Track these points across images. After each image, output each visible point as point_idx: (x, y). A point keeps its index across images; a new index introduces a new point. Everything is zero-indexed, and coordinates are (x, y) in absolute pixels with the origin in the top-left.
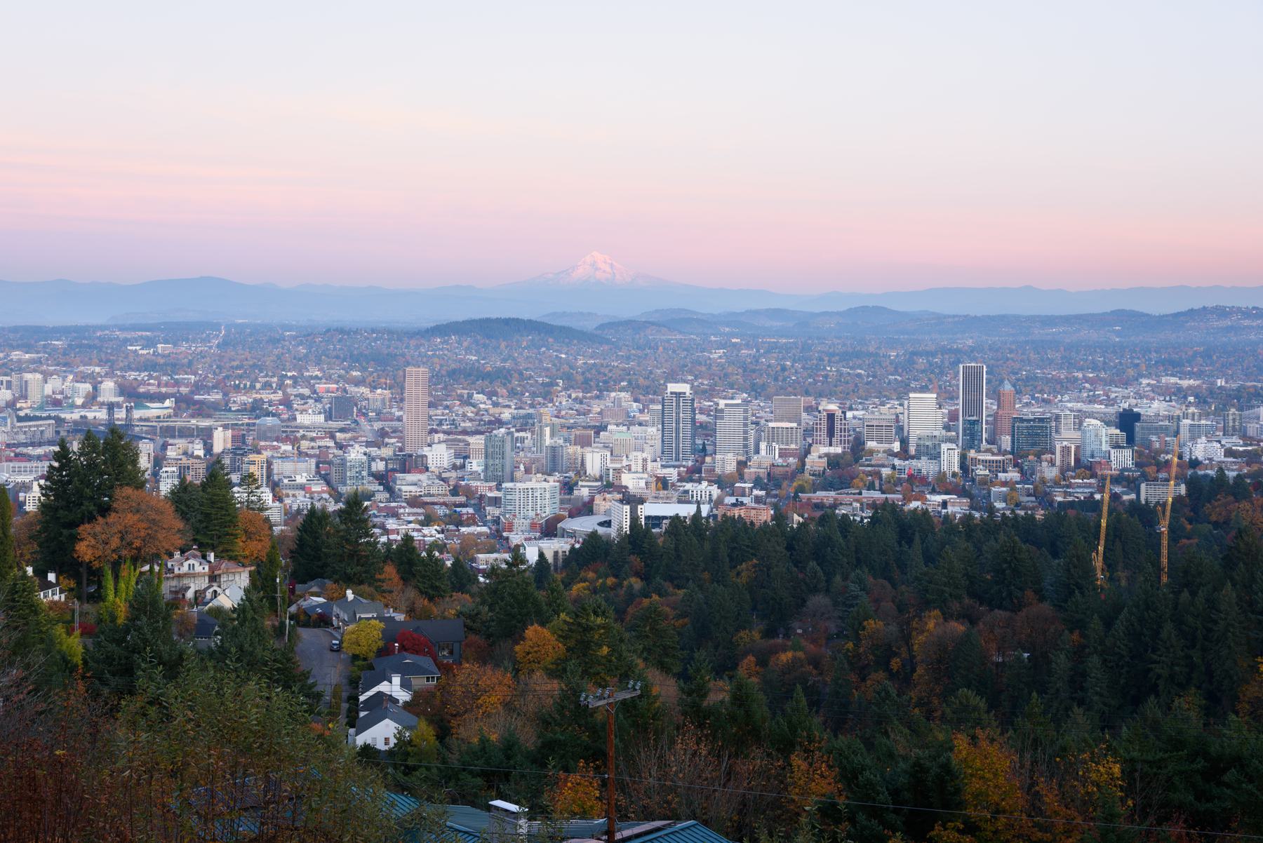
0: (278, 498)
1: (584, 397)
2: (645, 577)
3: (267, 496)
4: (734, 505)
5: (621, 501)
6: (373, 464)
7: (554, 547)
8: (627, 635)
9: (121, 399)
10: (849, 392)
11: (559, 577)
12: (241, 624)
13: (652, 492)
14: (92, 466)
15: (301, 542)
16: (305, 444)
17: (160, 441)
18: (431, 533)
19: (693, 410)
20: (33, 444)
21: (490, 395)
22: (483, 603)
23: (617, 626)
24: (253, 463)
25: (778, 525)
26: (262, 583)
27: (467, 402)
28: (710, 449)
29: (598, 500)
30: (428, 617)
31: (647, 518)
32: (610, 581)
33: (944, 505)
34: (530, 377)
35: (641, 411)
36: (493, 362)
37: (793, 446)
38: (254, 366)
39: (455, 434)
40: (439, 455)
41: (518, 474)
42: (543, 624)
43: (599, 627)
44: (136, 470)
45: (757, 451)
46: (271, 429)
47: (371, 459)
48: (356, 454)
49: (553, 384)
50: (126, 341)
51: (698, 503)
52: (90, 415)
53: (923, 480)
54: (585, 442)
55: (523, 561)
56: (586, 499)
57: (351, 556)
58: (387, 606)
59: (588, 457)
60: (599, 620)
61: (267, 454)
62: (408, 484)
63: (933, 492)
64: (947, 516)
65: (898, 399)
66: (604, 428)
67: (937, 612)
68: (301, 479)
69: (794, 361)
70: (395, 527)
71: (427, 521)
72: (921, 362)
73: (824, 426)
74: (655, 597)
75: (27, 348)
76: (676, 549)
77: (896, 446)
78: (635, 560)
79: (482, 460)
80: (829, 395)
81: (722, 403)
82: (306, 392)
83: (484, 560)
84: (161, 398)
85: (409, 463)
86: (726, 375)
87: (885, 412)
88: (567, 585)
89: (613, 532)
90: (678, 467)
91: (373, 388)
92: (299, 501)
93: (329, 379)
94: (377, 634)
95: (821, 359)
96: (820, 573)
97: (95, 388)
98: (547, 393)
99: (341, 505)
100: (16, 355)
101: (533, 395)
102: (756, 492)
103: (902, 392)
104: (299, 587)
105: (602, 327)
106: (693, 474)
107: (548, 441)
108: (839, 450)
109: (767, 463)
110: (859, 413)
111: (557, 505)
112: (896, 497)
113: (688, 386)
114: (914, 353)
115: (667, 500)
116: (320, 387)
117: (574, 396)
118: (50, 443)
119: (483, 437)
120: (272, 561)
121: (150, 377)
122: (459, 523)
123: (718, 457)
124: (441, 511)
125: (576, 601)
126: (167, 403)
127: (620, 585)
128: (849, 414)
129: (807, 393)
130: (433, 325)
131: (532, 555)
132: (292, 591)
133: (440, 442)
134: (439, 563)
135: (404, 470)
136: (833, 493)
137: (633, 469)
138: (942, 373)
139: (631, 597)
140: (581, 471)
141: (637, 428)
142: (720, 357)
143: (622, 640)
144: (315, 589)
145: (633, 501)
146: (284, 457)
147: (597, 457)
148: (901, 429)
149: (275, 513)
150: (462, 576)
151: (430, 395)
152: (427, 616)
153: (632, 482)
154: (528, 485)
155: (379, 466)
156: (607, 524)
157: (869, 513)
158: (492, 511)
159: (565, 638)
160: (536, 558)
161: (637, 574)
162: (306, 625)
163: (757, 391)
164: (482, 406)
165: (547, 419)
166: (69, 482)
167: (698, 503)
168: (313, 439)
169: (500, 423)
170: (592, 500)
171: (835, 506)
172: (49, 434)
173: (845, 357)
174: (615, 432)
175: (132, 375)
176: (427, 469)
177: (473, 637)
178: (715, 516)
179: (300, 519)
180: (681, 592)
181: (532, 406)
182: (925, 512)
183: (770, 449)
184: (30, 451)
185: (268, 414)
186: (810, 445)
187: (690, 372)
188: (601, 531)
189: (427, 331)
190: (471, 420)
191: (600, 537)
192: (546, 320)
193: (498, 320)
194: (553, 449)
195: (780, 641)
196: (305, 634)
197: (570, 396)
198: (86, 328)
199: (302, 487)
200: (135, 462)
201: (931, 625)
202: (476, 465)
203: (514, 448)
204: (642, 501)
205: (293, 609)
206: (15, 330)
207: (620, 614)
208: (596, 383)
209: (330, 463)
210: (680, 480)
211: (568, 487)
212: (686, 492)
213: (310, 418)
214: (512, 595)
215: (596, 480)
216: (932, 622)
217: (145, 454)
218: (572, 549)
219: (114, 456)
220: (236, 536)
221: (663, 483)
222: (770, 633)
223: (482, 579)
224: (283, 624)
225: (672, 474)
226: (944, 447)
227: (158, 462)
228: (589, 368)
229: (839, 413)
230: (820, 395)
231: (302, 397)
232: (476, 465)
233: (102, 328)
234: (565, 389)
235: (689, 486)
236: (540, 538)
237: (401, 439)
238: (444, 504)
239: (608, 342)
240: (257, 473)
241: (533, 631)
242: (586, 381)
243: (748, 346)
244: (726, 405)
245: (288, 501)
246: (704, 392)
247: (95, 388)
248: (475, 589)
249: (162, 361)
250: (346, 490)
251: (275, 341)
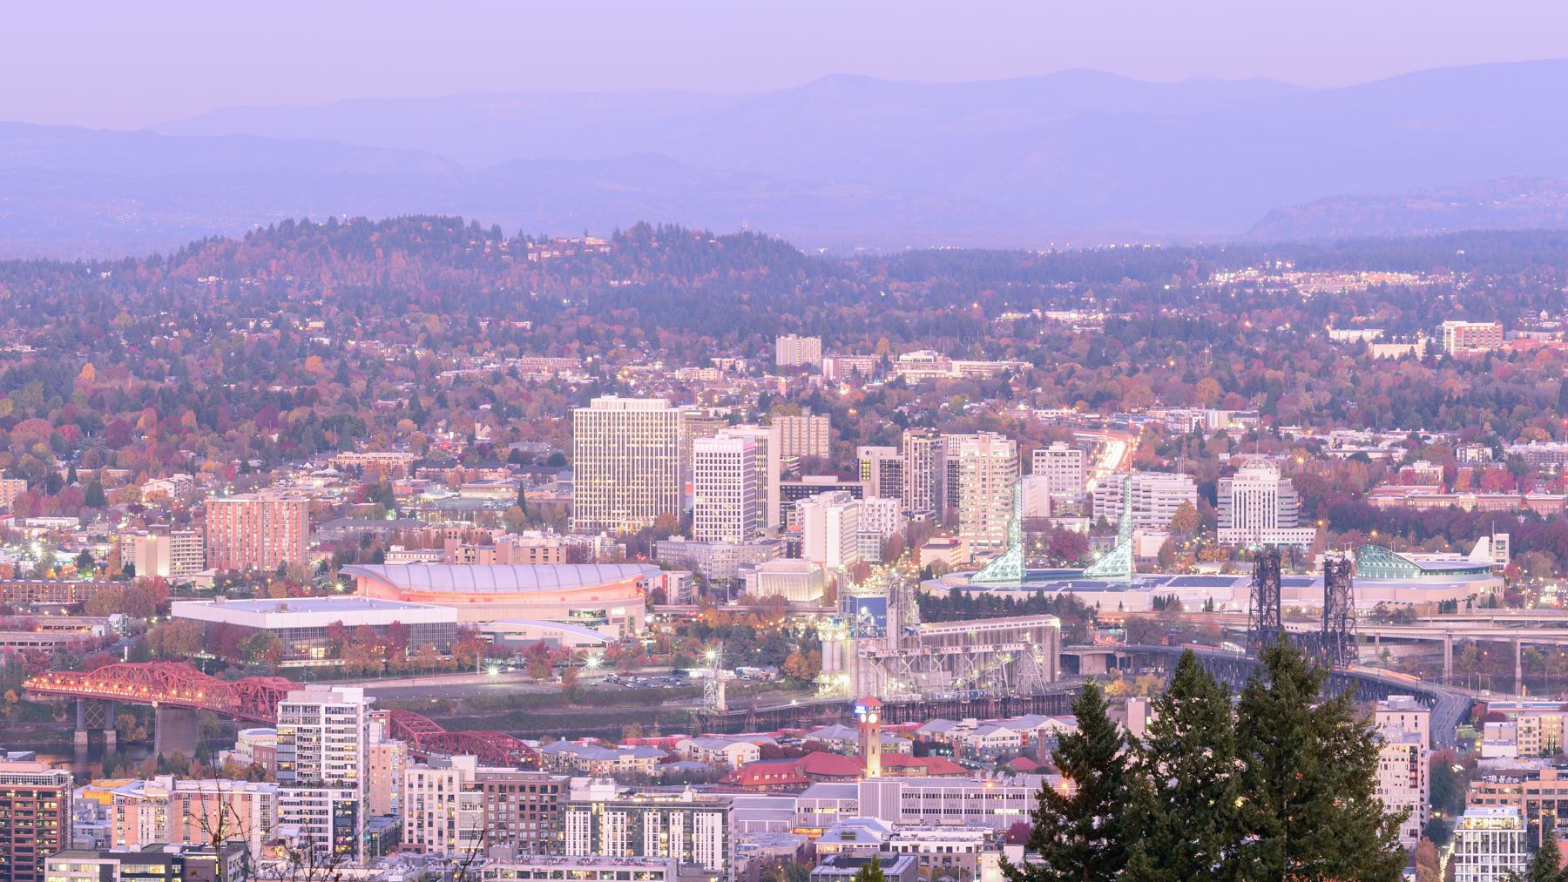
9: (1303, 537)
14: (1197, 793)
17: (1453, 698)
20: (979, 708)
44: (1371, 817)
50: (1324, 306)
52: (1192, 599)
75: (959, 337)
84: (1456, 530)
97: (1208, 493)
100: (915, 365)
118: (1046, 703)
121: (1416, 448)
126: (1483, 551)
166: (1117, 857)
172: (1040, 667)
175: (1345, 441)
184: (969, 732)
198: (1173, 261)
200: (1359, 783)
206: (912, 266)
217: (1400, 741)
219: (1280, 761)
227: (1447, 791)
233: (1235, 257)
247: (1208, 493)
249: (1459, 386)
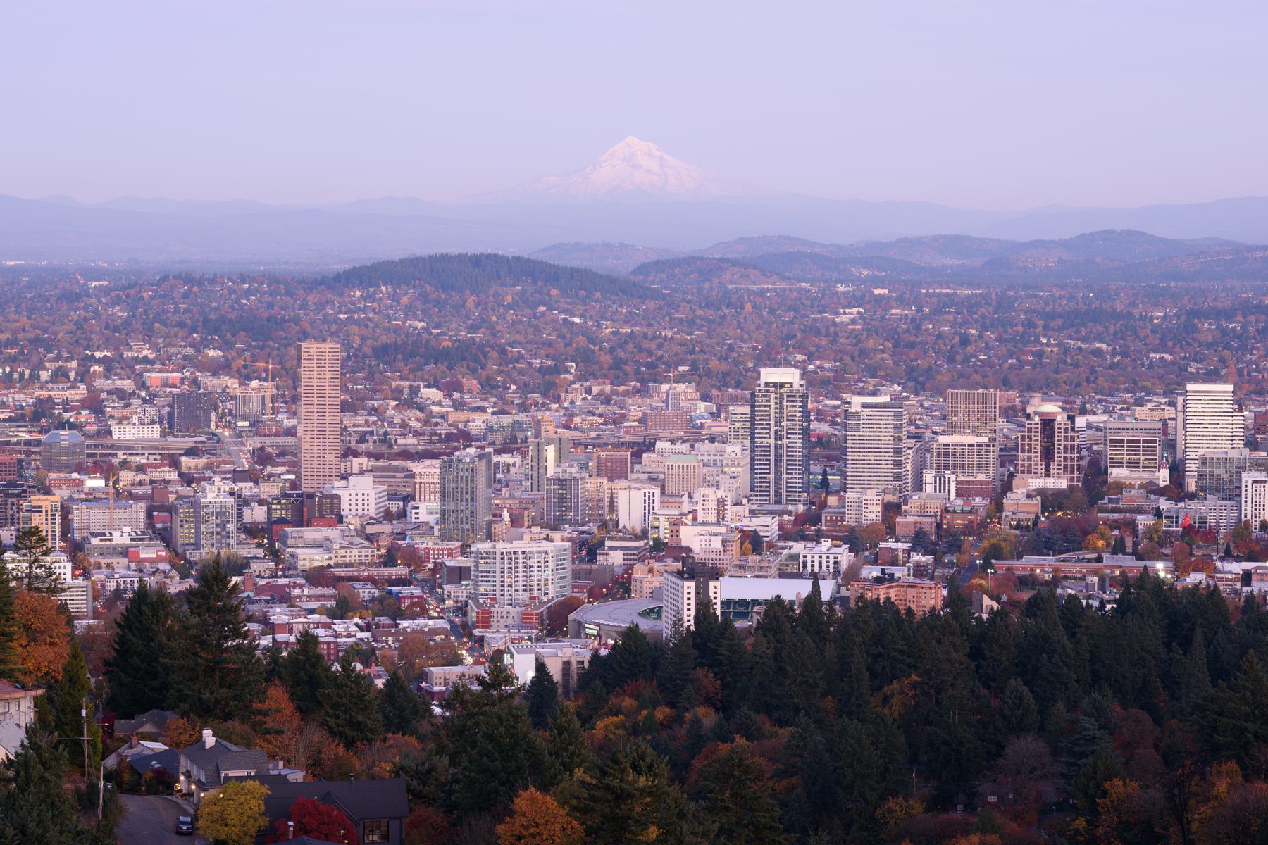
0: (82, 569)
1: (614, 393)
2: (723, 707)
3: (64, 567)
4: (878, 580)
5: (680, 574)
6: (247, 512)
7: (562, 655)
8: (691, 806)
10: (1078, 385)
11: (571, 705)
12: (22, 789)
13: (732, 558)
15: (123, 648)
16: (126, 477)
18: (349, 630)
19: (806, 415)
21: (449, 389)
22: (441, 750)
23: (674, 790)
24: (37, 509)
25: (955, 615)
26: (55, 717)
27: (411, 402)
28: (834, 479)
29: (639, 571)
30: (345, 776)
31: (726, 603)
32: (662, 713)
33: (1247, 578)
34: (519, 358)
35: (715, 416)
36: (452, 333)
37: (982, 477)
38: (36, 342)
39: (387, 456)
40: (361, 494)
41: (499, 528)
42: (544, 788)
43: (643, 792)
45: (919, 486)
46: (68, 451)
47: (243, 502)
48: (215, 493)
49: (559, 369)
51: (815, 577)
53: (1210, 535)
54: (616, 472)
55: (509, 680)
56: (619, 571)
57: (210, 670)
58: (273, 756)
59: (622, 497)
60: (642, 781)
61: (60, 494)
62: (310, 549)
63: (1228, 556)
64: (1250, 599)
65: (1165, 394)
66: (649, 446)
67: (1232, 766)
68: (121, 538)
69: (983, 328)
70: (285, 619)
71: (342, 610)
72: (1207, 327)
73: (1037, 444)
74: (740, 741)
76: (777, 656)
77: (1163, 477)
78: (705, 677)
79: (436, 506)
80: (1046, 388)
81: (856, 402)
82: (127, 385)
83: (440, 677)
85: (309, 508)
86: (864, 353)
87: (1148, 414)
88: (587, 719)
89: (665, 627)
90: (781, 513)
91: (245, 378)
92: (120, 576)
93: (165, 361)
94: (257, 805)
95: (1030, 324)
96: (1029, 699)
98: (549, 388)
99: (190, 583)
101: (525, 389)
102: (917, 558)
103: (1172, 384)
104: (121, 726)
105: (642, 269)
106: (805, 527)
107: (551, 470)
108: (1063, 484)
109: (936, 505)
110: (1099, 419)
111: (568, 582)
112: (1161, 569)
113: (797, 372)
114: (1195, 313)
115: (761, 572)
116: (153, 377)
117: (595, 390)
119: (437, 463)
120: (73, 679)
122: (397, 614)
123: (850, 496)
124: (365, 593)
125: (604, 747)
127: (679, 719)
128: (1081, 421)
129: (1006, 384)
130: (348, 266)
131: (523, 670)
132: (109, 733)
133: (362, 473)
134: (363, 682)
135: (300, 522)
136: (1051, 560)
137: (700, 519)
138: (1244, 348)
139: (698, 740)
140: (609, 526)
141: (706, 447)
142: (853, 321)
143: (682, 815)
144: (148, 728)
145: (699, 572)
146: (92, 499)
147: (638, 497)
148: (1172, 446)
149: (77, 596)
150: (403, 703)
151: (344, 389)
152: (341, 773)
153: (699, 541)
154: (518, 546)
155: (257, 514)
156: (654, 613)
157: (1113, 593)
158: (456, 592)
159: (584, 811)
160: (531, 674)
161: (708, 701)
162: (133, 790)
163: (918, 381)
164: (435, 409)
165: (548, 430)
167: (815, 577)
168: (140, 469)
169: (466, 437)
170: (629, 569)
171: (1055, 582)
173: (1074, 320)
174: (669, 455)
176: (340, 519)
177: (423, 810)
178: (845, 600)
179: (121, 607)
180: (786, 733)
181: (523, 408)
182: (1214, 592)
183: (941, 483)
185: (62, 425)
186: (1012, 475)
187: (801, 348)
188: (645, 625)
189: (338, 277)
190: (416, 434)
191: (644, 636)
192: (546, 258)
193: (461, 258)
194: (561, 482)
195: (958, 815)
196: (133, 805)
197: (589, 391)
199: (124, 552)
201: (1222, 787)
202: (426, 511)
203: (496, 485)
204: (716, 574)
205: (111, 762)
207: (680, 770)
208: (636, 367)
209: (171, 509)
210: (785, 535)
211: (588, 549)
212: (794, 557)
213: (135, 430)
214: (490, 738)
215: (636, 537)
216: (1224, 783)
218: (595, 656)
220: (10, 637)
221: (753, 542)
222: (940, 802)
223: (437, 710)
224: (93, 788)
225: (768, 526)
226: (1247, 478)
228: (622, 342)
229: (1061, 419)
230: (1029, 387)
231: (120, 394)
232: (426, 511)
234: (580, 378)
235: (798, 547)
236: (538, 639)
237: (295, 467)
238: (371, 580)
239: (655, 295)
240: (45, 528)
241: (527, 800)
242: (618, 364)
243: (902, 302)
244: (864, 405)
245: (98, 576)
246: (825, 382)
248: (425, 727)
250: (205, 553)
251: (73, 298)
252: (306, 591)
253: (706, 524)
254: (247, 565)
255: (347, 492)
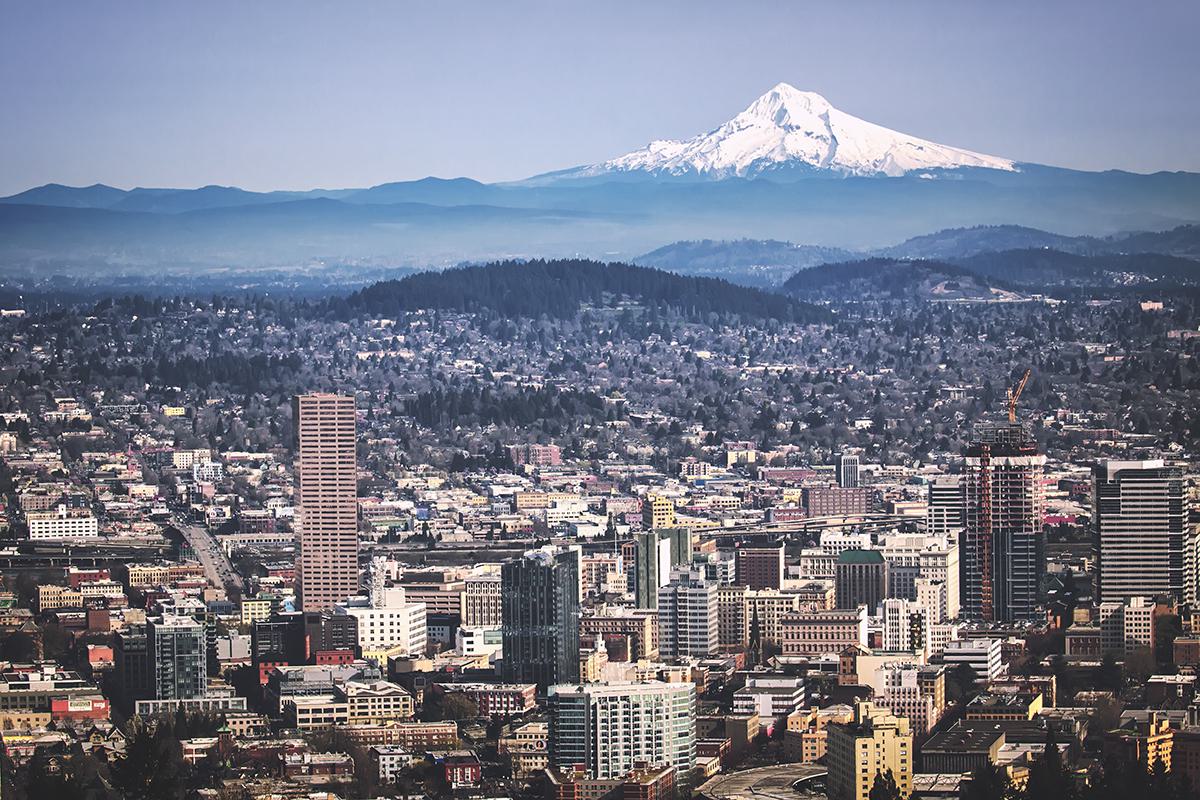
1: (761, 461)
105: (802, 279)
130: (370, 281)
252: (308, 758)
253: (894, 651)
254: (223, 722)
255: (366, 612)
